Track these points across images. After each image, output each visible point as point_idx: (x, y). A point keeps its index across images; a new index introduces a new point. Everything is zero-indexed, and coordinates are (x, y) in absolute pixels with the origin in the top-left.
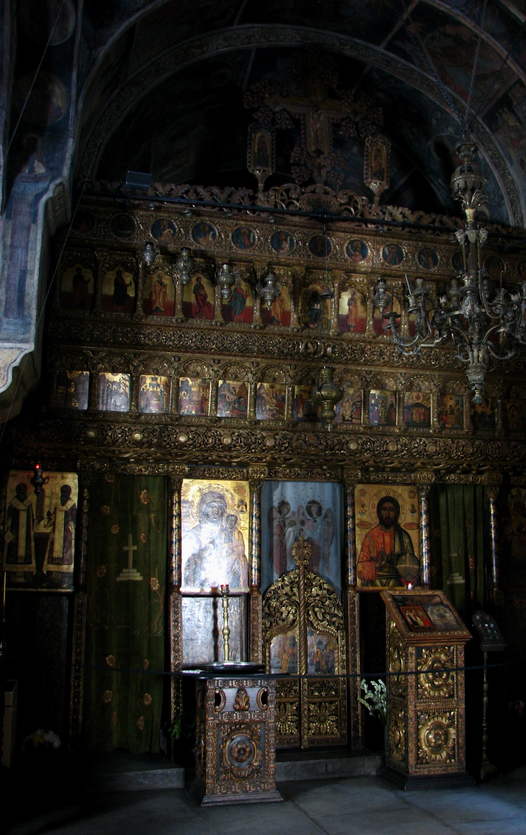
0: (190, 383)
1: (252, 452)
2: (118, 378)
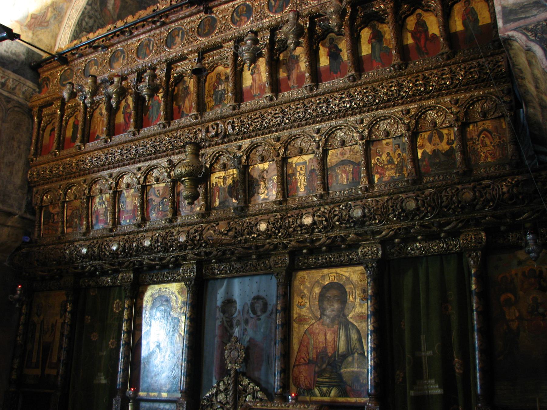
0: (126, 194)
1: (172, 252)
2: (77, 203)
